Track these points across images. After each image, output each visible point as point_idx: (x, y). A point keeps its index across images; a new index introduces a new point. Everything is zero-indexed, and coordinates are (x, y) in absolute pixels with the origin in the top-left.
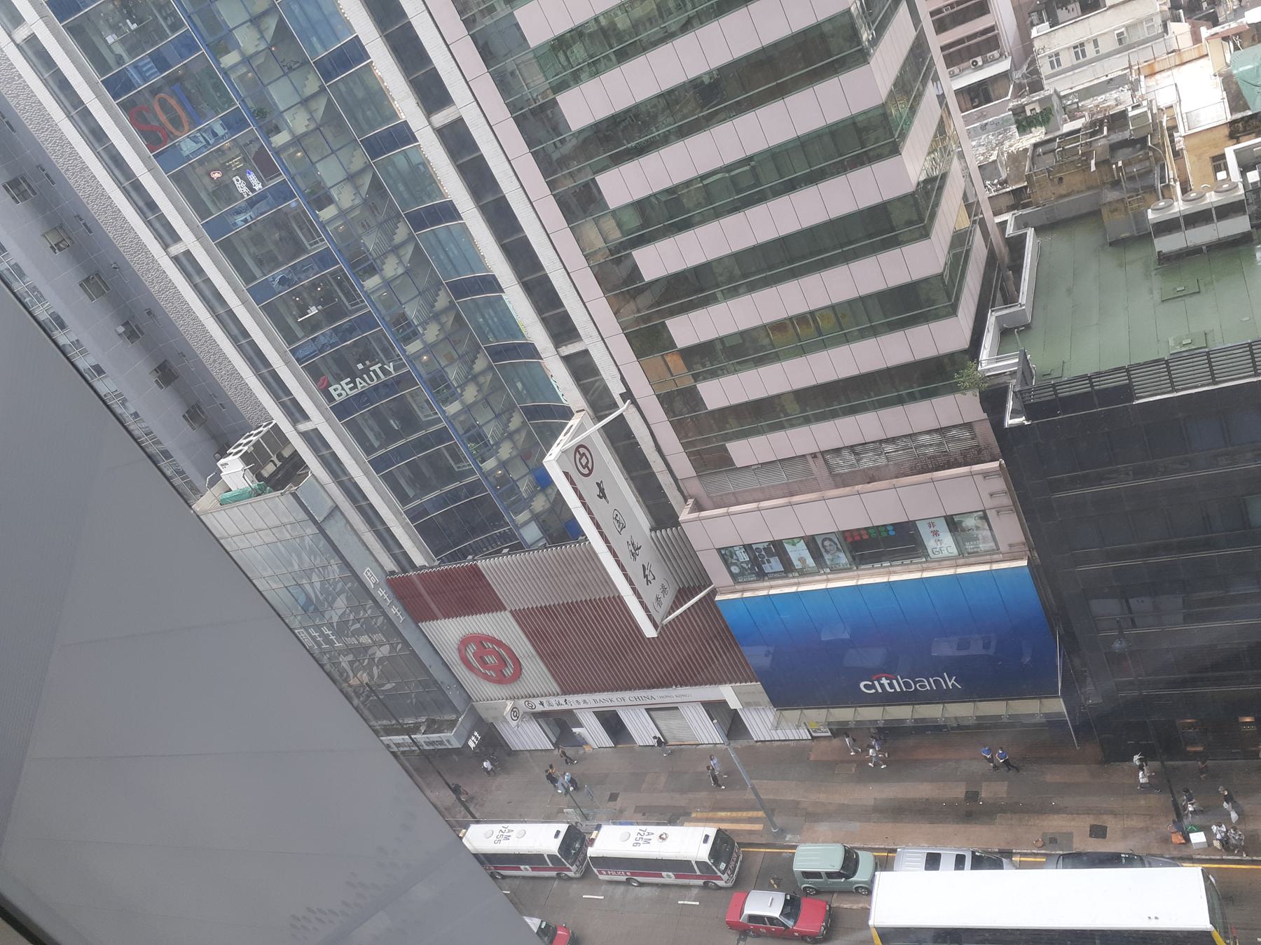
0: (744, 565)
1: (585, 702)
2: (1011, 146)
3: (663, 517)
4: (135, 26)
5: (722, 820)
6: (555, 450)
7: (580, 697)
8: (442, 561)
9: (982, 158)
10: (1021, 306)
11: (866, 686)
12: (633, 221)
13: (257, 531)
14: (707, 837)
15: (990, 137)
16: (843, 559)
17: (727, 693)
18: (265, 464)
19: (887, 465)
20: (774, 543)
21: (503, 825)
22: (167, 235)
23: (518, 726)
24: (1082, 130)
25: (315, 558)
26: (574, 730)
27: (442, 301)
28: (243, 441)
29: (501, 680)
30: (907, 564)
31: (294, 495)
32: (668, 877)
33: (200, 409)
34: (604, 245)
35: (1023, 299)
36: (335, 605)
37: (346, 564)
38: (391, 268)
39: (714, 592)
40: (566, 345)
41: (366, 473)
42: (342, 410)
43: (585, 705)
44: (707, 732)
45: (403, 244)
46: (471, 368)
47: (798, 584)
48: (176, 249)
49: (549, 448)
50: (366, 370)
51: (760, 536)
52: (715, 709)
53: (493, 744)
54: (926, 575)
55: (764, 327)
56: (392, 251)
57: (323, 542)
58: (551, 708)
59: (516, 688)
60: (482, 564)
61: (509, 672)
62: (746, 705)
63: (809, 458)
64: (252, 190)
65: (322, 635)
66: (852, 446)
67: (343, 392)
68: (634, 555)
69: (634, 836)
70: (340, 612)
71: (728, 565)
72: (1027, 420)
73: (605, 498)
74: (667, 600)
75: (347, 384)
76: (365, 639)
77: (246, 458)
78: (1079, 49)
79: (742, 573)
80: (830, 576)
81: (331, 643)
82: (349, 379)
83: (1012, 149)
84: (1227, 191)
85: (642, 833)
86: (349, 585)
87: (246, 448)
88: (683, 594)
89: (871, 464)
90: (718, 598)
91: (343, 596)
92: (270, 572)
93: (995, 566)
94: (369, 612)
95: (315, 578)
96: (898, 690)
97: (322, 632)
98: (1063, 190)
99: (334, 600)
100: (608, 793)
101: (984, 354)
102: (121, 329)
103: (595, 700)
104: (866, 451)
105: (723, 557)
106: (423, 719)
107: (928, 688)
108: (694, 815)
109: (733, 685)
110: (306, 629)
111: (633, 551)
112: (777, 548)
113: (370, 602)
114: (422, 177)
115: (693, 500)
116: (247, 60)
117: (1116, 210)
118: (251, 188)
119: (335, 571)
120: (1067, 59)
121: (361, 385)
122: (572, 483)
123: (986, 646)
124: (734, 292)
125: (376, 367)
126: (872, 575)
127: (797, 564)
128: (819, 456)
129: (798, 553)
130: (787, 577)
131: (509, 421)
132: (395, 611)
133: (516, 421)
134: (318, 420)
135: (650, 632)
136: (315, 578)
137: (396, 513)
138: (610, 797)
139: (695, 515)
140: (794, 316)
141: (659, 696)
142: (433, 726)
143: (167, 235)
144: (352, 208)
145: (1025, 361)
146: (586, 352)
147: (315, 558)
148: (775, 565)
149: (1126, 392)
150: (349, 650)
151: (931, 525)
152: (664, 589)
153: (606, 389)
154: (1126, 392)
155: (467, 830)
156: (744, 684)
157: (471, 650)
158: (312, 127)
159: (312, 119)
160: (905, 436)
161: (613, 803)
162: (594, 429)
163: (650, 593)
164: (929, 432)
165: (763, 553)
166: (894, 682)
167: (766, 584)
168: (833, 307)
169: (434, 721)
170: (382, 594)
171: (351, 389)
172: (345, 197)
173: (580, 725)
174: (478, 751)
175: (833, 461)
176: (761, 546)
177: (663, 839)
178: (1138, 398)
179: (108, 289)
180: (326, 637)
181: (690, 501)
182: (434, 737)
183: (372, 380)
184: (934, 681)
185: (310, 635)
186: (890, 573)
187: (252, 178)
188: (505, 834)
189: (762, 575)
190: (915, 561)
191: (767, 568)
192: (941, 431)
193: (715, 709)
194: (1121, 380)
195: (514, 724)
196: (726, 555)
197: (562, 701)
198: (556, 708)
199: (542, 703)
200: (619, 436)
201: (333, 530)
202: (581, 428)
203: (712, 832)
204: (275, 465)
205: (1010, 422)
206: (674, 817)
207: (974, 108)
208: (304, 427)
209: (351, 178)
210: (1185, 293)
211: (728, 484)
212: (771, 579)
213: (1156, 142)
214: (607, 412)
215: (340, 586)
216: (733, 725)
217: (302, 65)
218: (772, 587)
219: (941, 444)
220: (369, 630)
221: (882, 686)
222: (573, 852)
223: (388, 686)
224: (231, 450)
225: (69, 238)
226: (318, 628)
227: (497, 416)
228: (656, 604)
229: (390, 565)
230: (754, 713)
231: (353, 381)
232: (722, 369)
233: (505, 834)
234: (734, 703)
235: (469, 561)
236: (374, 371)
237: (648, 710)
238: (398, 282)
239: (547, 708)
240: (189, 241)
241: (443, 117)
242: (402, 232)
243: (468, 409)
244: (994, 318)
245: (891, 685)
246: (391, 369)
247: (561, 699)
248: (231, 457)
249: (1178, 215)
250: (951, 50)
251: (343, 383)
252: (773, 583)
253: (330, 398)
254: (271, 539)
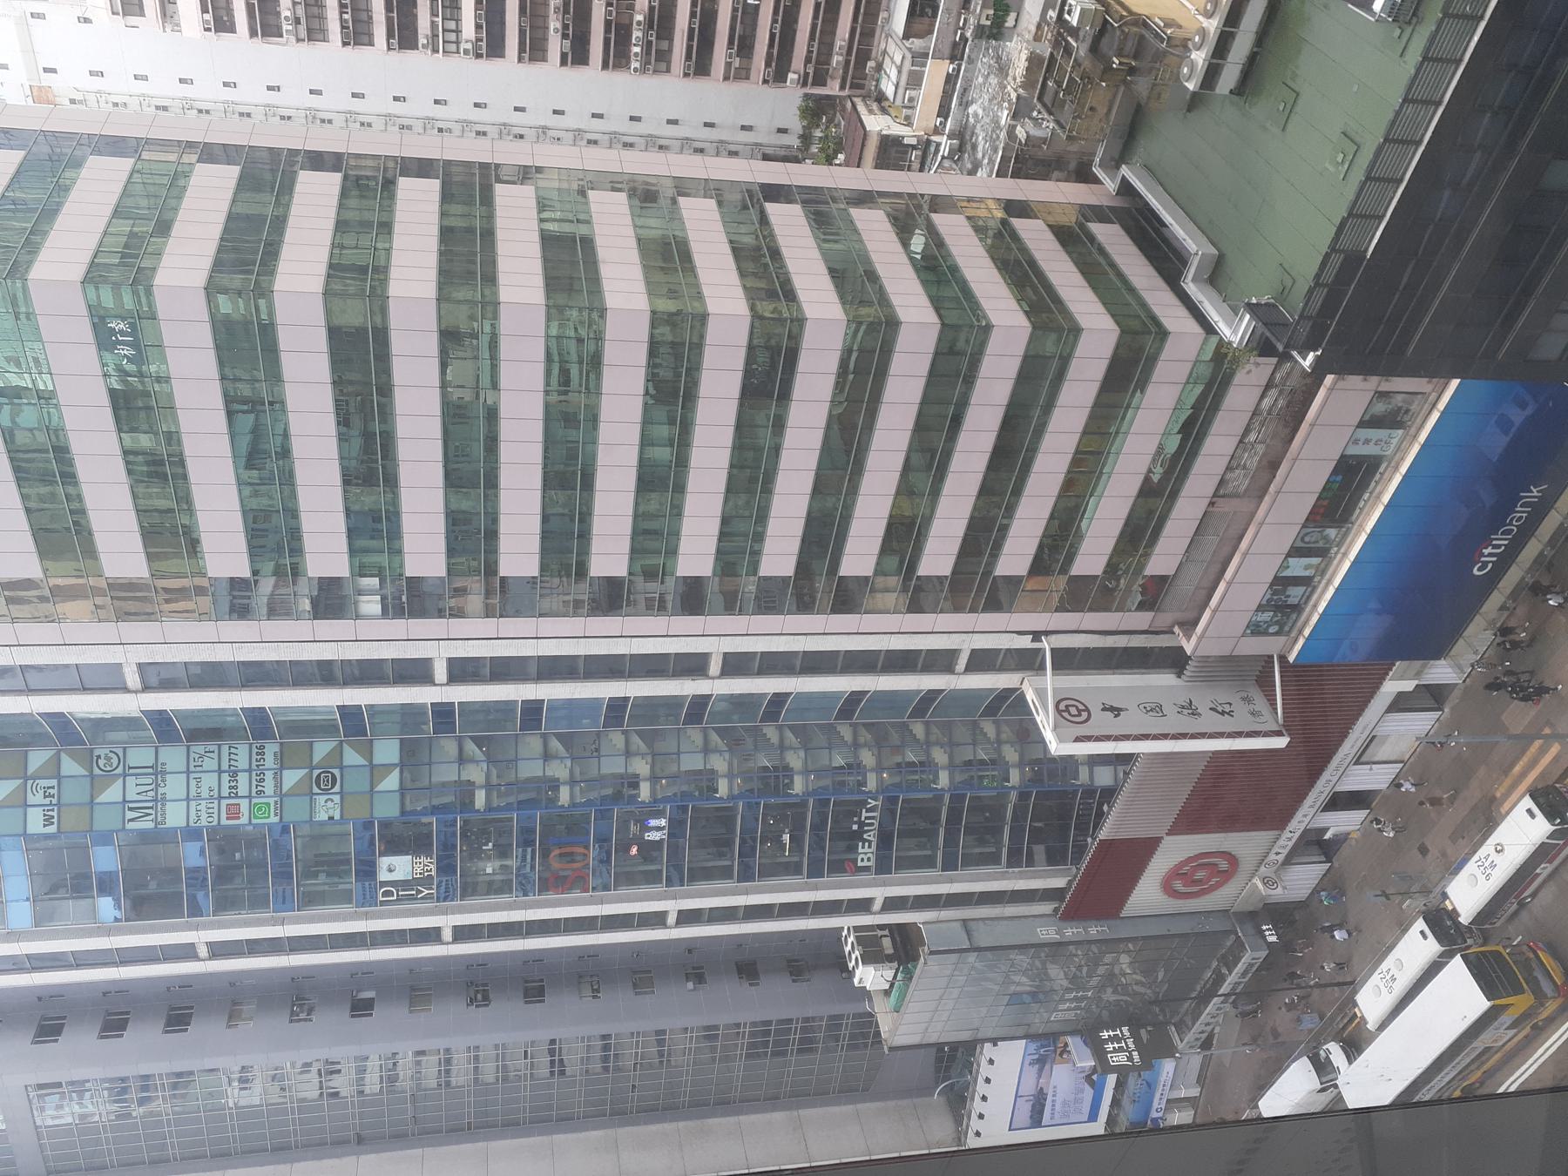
0: (1276, 619)
1: (1305, 816)
2: (1015, 79)
3: (1175, 660)
4: (490, 844)
5: (1523, 775)
6: (1049, 735)
7: (1299, 815)
8: (1077, 860)
9: (1006, 104)
10: (1197, 254)
11: (1479, 570)
12: (892, 562)
13: (941, 998)
14: (1529, 811)
15: (985, 60)
16: (1332, 533)
17: (1392, 687)
18: (881, 945)
19: (1268, 446)
20: (1272, 585)
21: (1377, 972)
22: (658, 920)
23: (1285, 888)
24: (1055, 53)
25: (1000, 968)
26: (1326, 837)
27: (845, 731)
28: (848, 948)
29: (1227, 876)
30: (1380, 479)
31: (932, 953)
32: (1544, 870)
33: (796, 961)
34: (896, 594)
35: (1191, 246)
36: (1052, 976)
37: (1022, 948)
38: (795, 760)
39: (1283, 659)
40: (956, 664)
41: (951, 881)
42: (883, 866)
43: (1307, 816)
44: (1421, 723)
45: (782, 739)
46: (918, 741)
47: (1329, 582)
48: (672, 919)
49: (1043, 741)
50: (861, 824)
51: (1258, 592)
52: (1401, 704)
53: (1281, 914)
54: (1404, 469)
55: (1060, 497)
56: (782, 752)
57: (989, 954)
58: (1289, 848)
59: (1246, 866)
60: (1103, 834)
61: (1224, 865)
62: (1418, 675)
63: (1211, 509)
64: (663, 828)
65: (1071, 1000)
66: (1227, 468)
67: (869, 855)
68: (1195, 714)
69: (1478, 873)
70: (1062, 975)
71: (1265, 633)
72: (1315, 350)
73: (1121, 710)
74: (1260, 703)
75: (863, 848)
76: (1101, 970)
77: (867, 959)
79: (1281, 625)
80: (1342, 550)
81: (1084, 998)
82: (860, 844)
83: (1018, 80)
84: (1215, 8)
85: (1480, 863)
86: (1043, 955)
87: (857, 953)
88: (1265, 683)
89: (1257, 458)
90: (1291, 659)
91: (1049, 966)
92: (984, 1010)
93: (1441, 405)
94: (1079, 953)
95: (1017, 978)
96: (1506, 542)
97: (1068, 1000)
98: (1102, 110)
99: (1046, 974)
100: (1415, 852)
101: (1225, 330)
102: (690, 985)
103: (1312, 807)
104: (1241, 457)
105: (1253, 633)
106: (1215, 964)
107: (1524, 515)
108: (1498, 795)
109: (1388, 677)
110: (1056, 1010)
111: (1190, 711)
112: (1281, 583)
113: (1071, 947)
114: (742, 703)
115: (1176, 627)
116: (572, 782)
117: (1160, 94)
118: (659, 829)
119: (1022, 960)
121: (871, 836)
122: (1088, 738)
123: (1523, 406)
124: (1010, 511)
125: (864, 814)
126: (1369, 514)
127: (1307, 573)
128: (1215, 499)
129: (1298, 567)
130: (1315, 588)
131: (986, 734)
132: (1094, 930)
133: (989, 728)
134: (879, 894)
135: (1281, 742)
136: (1017, 978)
137: (1003, 876)
138: (1422, 853)
139: (1194, 639)
140: (1070, 467)
141: (1349, 748)
142: (1230, 961)
143: (658, 920)
144: (730, 765)
147: (1000, 968)
148: (1295, 593)
149: (1353, 259)
150: (1101, 988)
151: (1356, 442)
152: (1247, 700)
154: (1353, 259)
155: (1357, 1005)
156: (1394, 668)
157: (1178, 885)
158: (649, 759)
159: (643, 755)
160: (1251, 419)
161: (1429, 856)
162: (1049, 680)
163: (1242, 720)
164: (1263, 396)
165: (1275, 597)
166: (1494, 542)
167: (1308, 609)
168: (1085, 433)
169: (1224, 957)
170: (1071, 932)
171: (870, 847)
172: (719, 763)
173: (1325, 830)
174: (1281, 931)
175: (1229, 489)
176: (1268, 596)
177: (1502, 851)
178: (1367, 249)
179: (650, 972)
180: (1076, 999)
181: (1176, 629)
182: (1240, 967)
183: (872, 824)
184: (1521, 506)
185: (1062, 1010)
186: (1378, 497)
187: (653, 823)
188: (1388, 978)
189: (1297, 608)
190: (1381, 470)
191: (1292, 601)
192: (1268, 387)
193: (1401, 704)
194: (1337, 260)
195: (1279, 890)
196: (1256, 630)
197: (1290, 835)
198: (1291, 844)
199: (1277, 854)
200: (1067, 661)
201: (984, 940)
202: (1041, 693)
203: (1528, 802)
204: (885, 936)
206: (1486, 819)
207: (935, 16)
208: (877, 906)
209: (707, 750)
210: (1289, 107)
212: (1306, 603)
213: (1117, 17)
214: (1040, 658)
215: (1038, 963)
216: (1432, 696)
217: (599, 738)
218: (1315, 606)
219: (1281, 392)
220: (1095, 962)
221: (1490, 555)
222: (1452, 931)
223: (1161, 975)
224: (851, 965)
225: (592, 976)
226: (1063, 1000)
227: (974, 744)
228: (1258, 720)
229: (1046, 908)
230: (1433, 671)
231: (864, 841)
232: (1071, 546)
233: (1388, 978)
234: (1408, 686)
235: (1092, 843)
236: (866, 818)
237: (1357, 762)
238: (809, 762)
239: (1285, 852)
240: (672, 907)
241: (715, 667)
242: (771, 732)
243: (951, 766)
244: (1191, 285)
245: (1499, 546)
246: (874, 803)
247: (1286, 834)
248: (858, 973)
249: (1207, 63)
250: (862, 11)
251: (860, 850)
252: (1312, 603)
253: (867, 869)
254: (956, 992)
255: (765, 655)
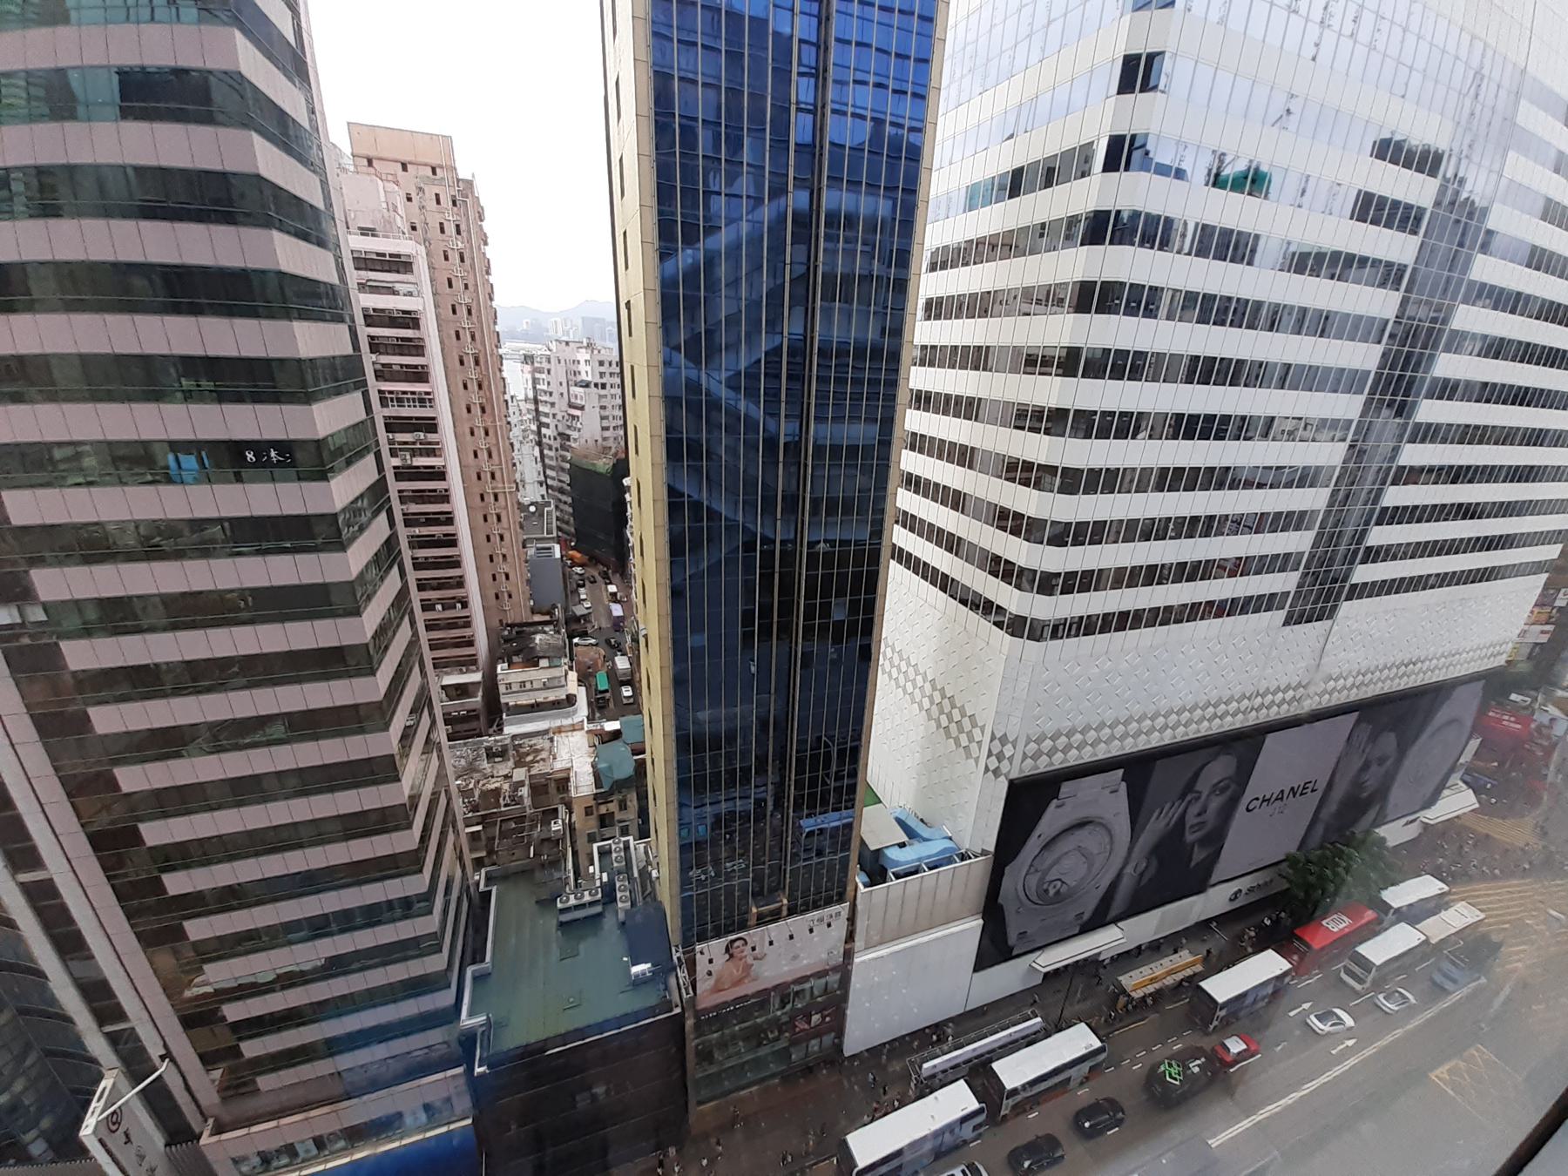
35: (488, 958)
78: (523, 684)
120: (515, 688)
128: (336, 1076)
139: (215, 1138)
145: (488, 1018)
146: (133, 1029)
153: (143, 1049)
181: (211, 1121)
205: (478, 1070)
211: (250, 1105)
255: (64, 910)
